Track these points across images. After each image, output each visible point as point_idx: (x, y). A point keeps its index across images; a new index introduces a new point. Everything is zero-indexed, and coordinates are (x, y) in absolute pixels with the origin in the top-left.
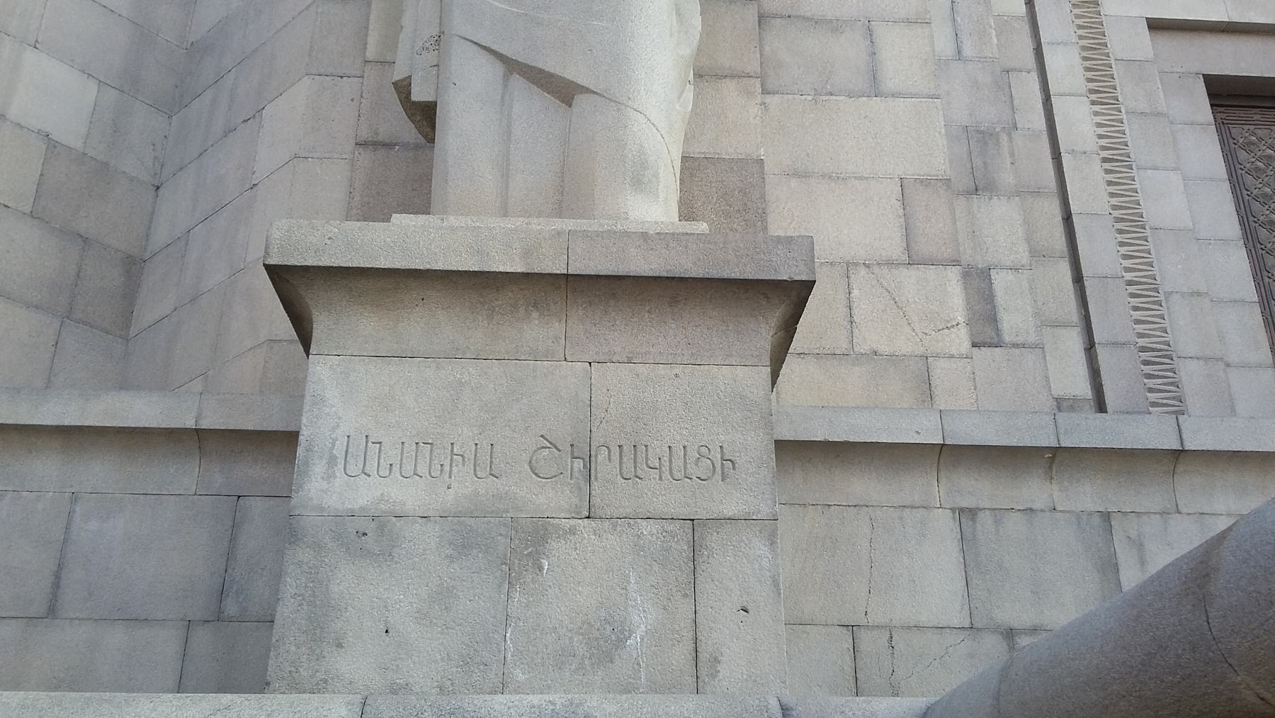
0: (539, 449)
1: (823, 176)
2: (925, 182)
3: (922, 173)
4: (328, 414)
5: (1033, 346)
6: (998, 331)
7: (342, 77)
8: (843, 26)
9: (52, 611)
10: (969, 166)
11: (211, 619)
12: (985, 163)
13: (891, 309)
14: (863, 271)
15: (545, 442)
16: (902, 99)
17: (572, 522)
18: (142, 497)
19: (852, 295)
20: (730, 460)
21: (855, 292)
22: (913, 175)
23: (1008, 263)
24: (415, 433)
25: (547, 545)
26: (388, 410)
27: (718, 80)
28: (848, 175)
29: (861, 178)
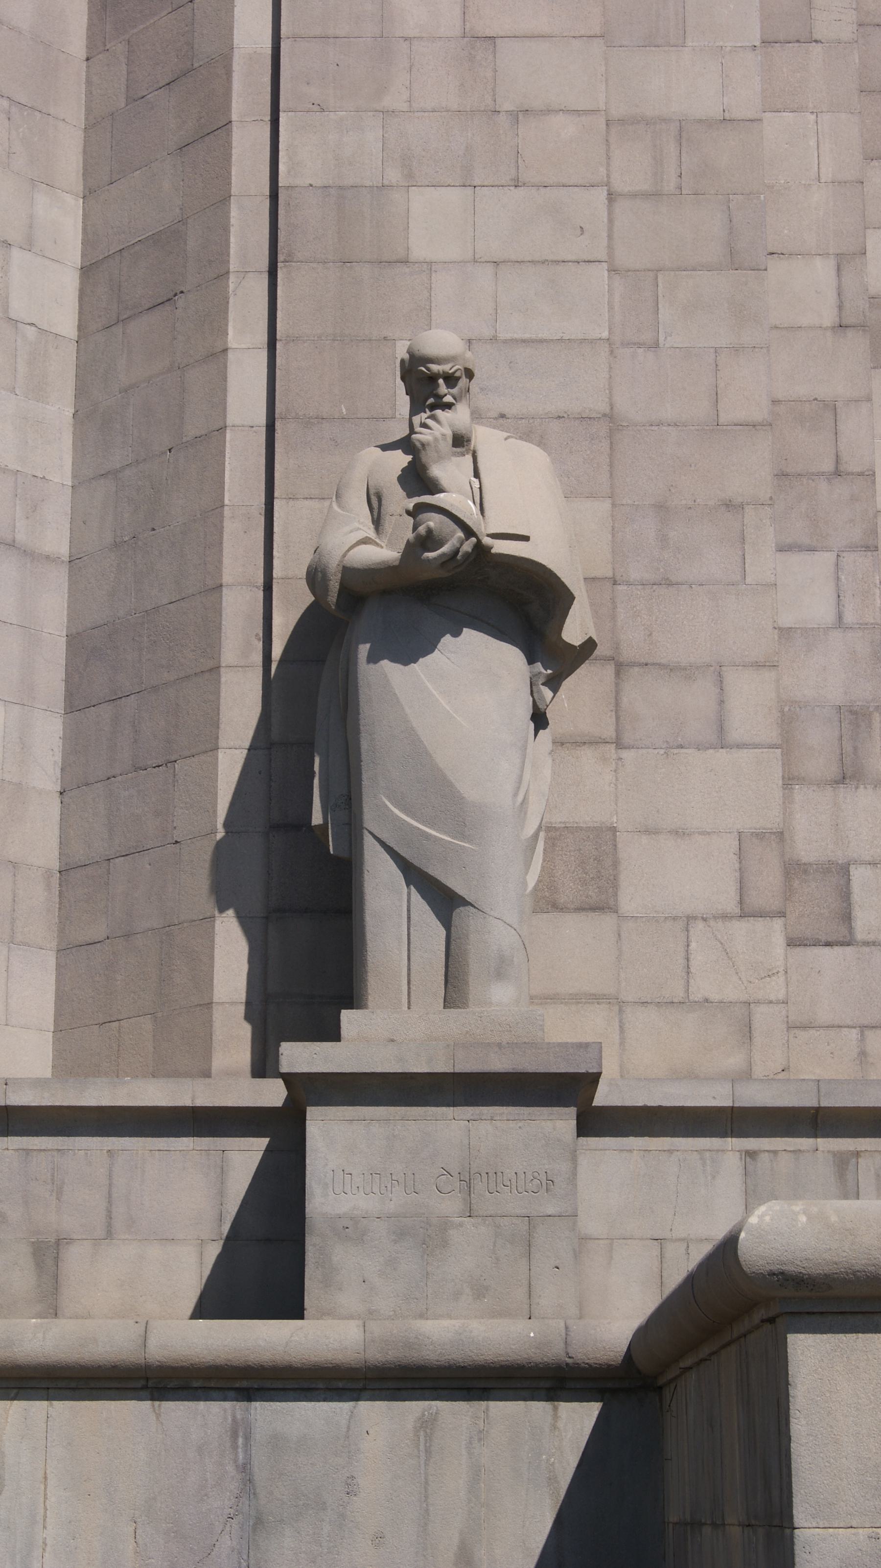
2: (760, 836)
3: (758, 827)
6: (851, 929)
8: (696, 673)
10: (838, 752)
11: (215, 1239)
12: (855, 749)
13: (723, 959)
14: (700, 925)
16: (745, 751)
18: (157, 1152)
19: (690, 948)
21: (693, 945)
25: (447, 1234)
27: (578, 748)
28: (692, 831)
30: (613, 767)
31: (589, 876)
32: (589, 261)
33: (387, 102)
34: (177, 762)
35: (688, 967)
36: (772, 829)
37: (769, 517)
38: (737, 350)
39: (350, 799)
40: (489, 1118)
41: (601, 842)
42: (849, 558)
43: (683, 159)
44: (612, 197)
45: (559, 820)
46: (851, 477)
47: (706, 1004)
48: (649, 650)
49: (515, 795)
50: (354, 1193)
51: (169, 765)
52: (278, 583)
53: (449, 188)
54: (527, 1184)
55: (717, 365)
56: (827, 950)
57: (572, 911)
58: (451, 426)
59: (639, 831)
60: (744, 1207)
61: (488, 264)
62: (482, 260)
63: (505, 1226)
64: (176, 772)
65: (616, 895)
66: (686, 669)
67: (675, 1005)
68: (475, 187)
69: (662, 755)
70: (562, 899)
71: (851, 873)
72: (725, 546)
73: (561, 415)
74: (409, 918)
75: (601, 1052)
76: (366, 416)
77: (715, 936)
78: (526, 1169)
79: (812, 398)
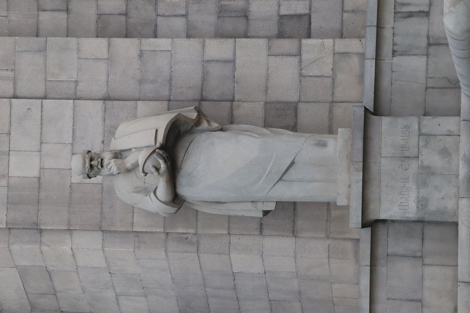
0: (402, 168)
1: (267, 82)
2: (269, 48)
4: (394, 214)
5: (311, 3)
6: (305, 15)
7: (230, 243)
9: (420, 301)
10: (236, 18)
11: (422, 259)
12: (234, 11)
14: (303, 71)
16: (236, 52)
17: (419, 161)
21: (311, 74)
23: (277, 8)
27: (234, 116)
28: (267, 73)
29: (268, 69)
30: (242, 103)
32: (42, 106)
34: (233, 271)
35: (320, 76)
36: (267, 43)
37: (145, 40)
38: (79, 50)
39: (253, 201)
40: (380, 149)
41: (270, 108)
42: (160, 12)
44: (15, 97)
45: (261, 124)
46: (128, 9)
47: (334, 70)
48: (196, 88)
49: (256, 137)
51: (234, 275)
52: (166, 230)
53: (10, 161)
56: (312, 24)
57: (297, 120)
58: (110, 159)
60: (414, 56)
61: (42, 146)
62: (40, 148)
63: (423, 144)
64: (238, 272)
65: (291, 103)
66: (204, 74)
67: (334, 81)
68: (10, 150)
69: (237, 84)
70: (292, 124)
71: (283, 14)
72: (157, 58)
73: (103, 119)
76: (101, 195)
78: (400, 136)
79: (96, 23)
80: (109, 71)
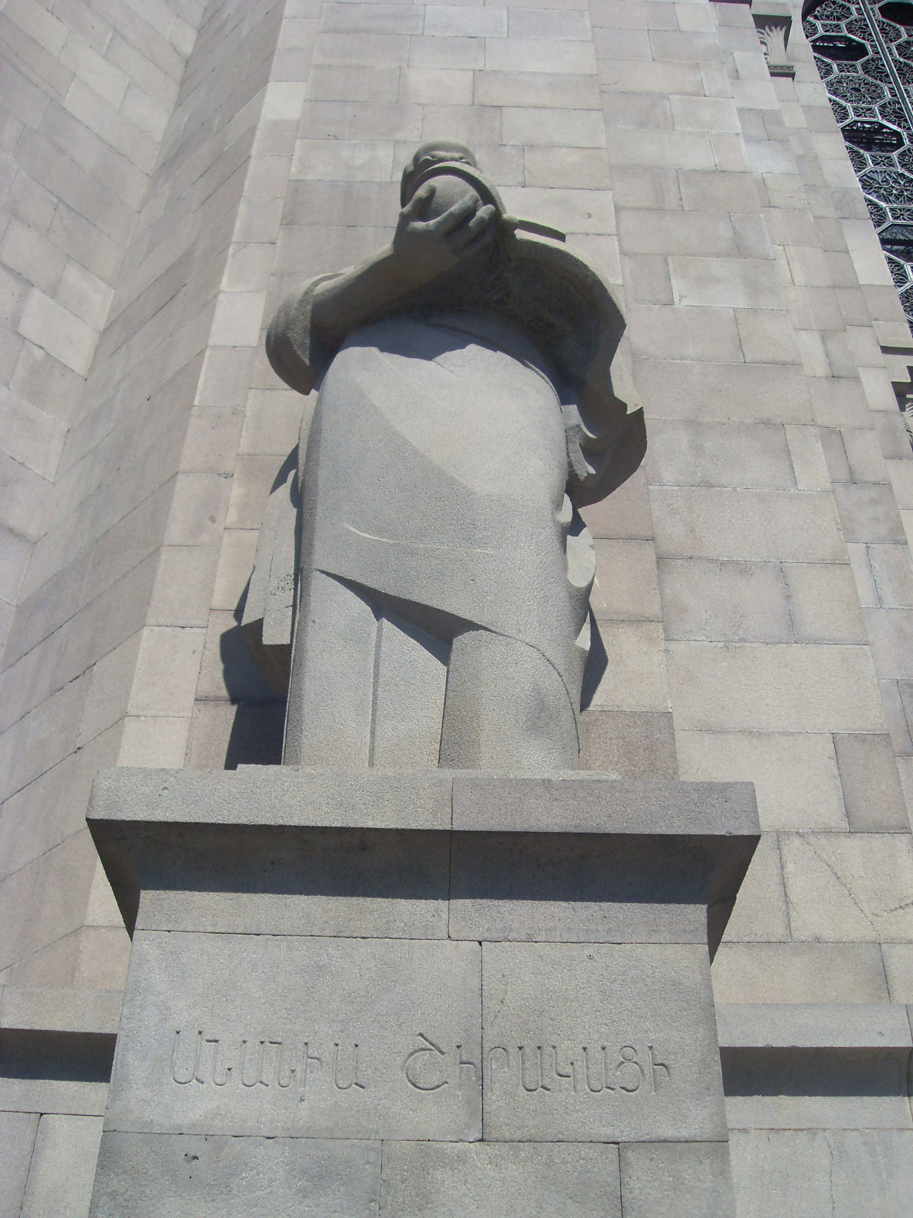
0: (416, 1051)
10: (903, 723)
14: (797, 842)
15: (425, 1042)
16: (826, 646)
20: (663, 1065)
21: (790, 867)
22: (846, 729)
24: (260, 1029)
26: (227, 1000)
28: (771, 731)
29: (784, 734)
31: (639, 768)
33: (400, 136)
38: (755, 311)
43: (682, 190)
50: (219, 1081)
54: (611, 1073)
55: (736, 320)
59: (700, 730)
67: (774, 945)
74: (376, 676)
75: (754, 799)
77: (819, 855)
78: (607, 1040)
80: (711, 362)
